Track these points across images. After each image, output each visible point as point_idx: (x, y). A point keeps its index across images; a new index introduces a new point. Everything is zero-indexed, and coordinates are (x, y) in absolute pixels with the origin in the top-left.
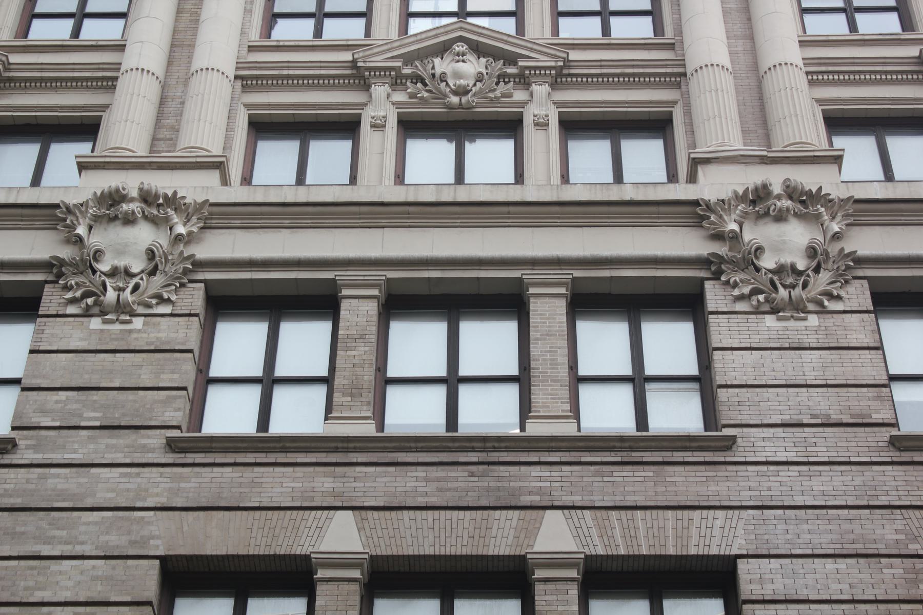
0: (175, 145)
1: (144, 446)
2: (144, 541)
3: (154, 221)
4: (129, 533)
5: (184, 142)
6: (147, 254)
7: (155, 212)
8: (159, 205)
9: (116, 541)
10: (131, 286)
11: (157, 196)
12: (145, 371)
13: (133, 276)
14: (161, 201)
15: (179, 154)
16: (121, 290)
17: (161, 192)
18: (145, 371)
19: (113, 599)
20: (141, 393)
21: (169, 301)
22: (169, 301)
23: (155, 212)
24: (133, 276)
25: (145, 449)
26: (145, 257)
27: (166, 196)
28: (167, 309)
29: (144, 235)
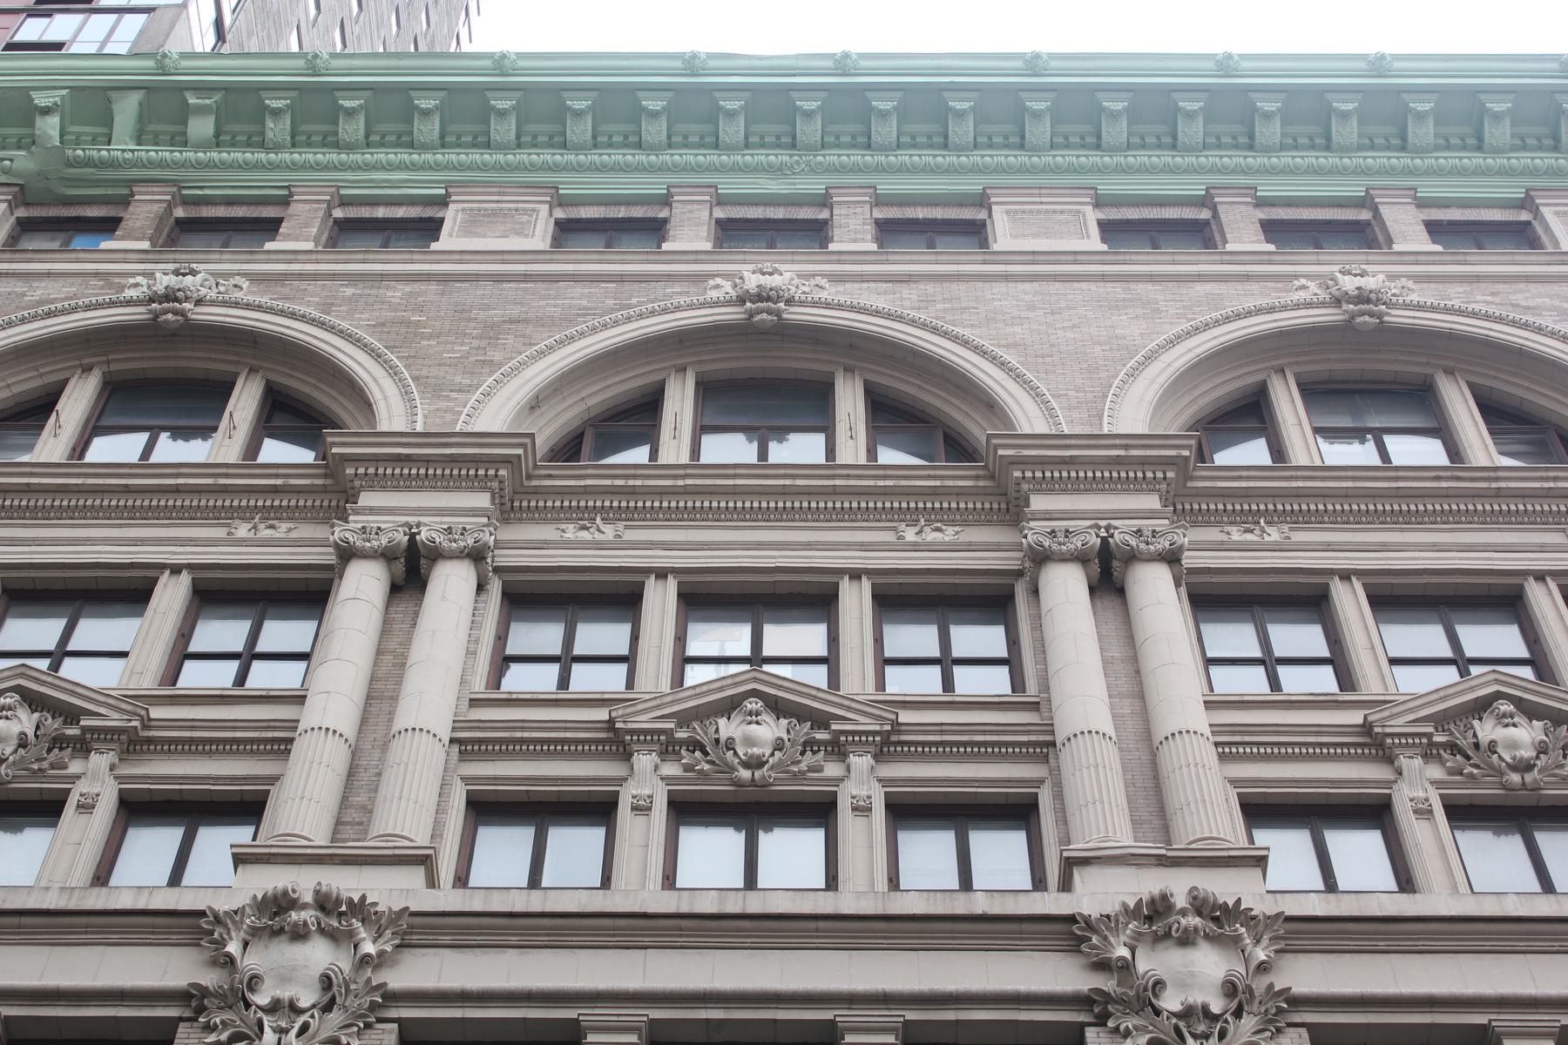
0: (366, 832)
3: (332, 936)
5: (377, 828)
6: (322, 981)
7: (336, 924)
8: (341, 914)
10: (297, 1026)
11: (338, 902)
13: (301, 1012)
14: (344, 908)
15: (370, 845)
16: (283, 1031)
17: (345, 895)
23: (336, 924)
24: (301, 1012)
26: (318, 986)
27: (351, 900)
29: (318, 956)
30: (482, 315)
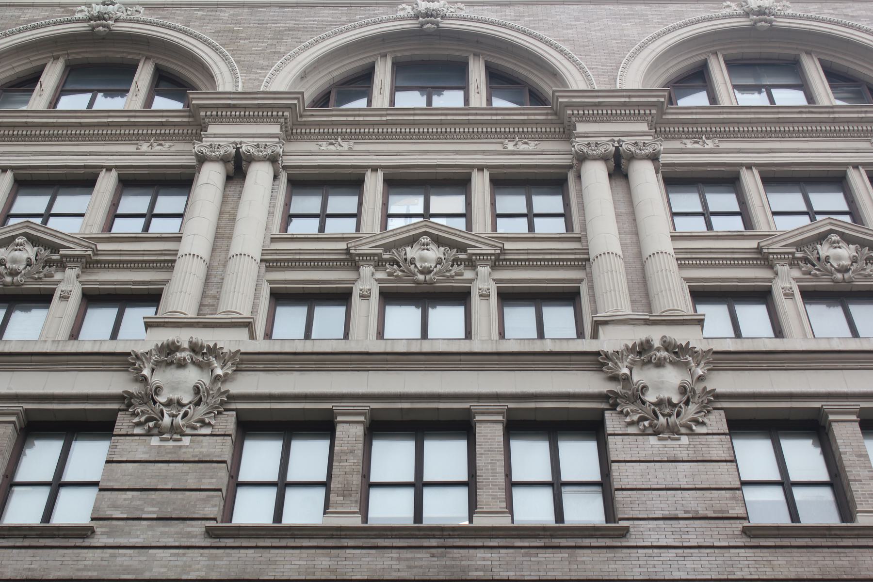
0: (216, 310)
1: (189, 533)
3: (199, 365)
5: (222, 308)
6: (194, 390)
7: (201, 359)
8: (203, 354)
10: (182, 413)
11: (202, 347)
12: (191, 477)
13: (183, 406)
14: (205, 351)
15: (219, 317)
16: (174, 416)
17: (205, 344)
18: (191, 477)
20: (187, 493)
21: (209, 424)
22: (209, 424)
23: (201, 359)
24: (183, 406)
25: (190, 535)
26: (192, 392)
27: (209, 347)
28: (207, 431)
29: (192, 376)
30: (273, 26)
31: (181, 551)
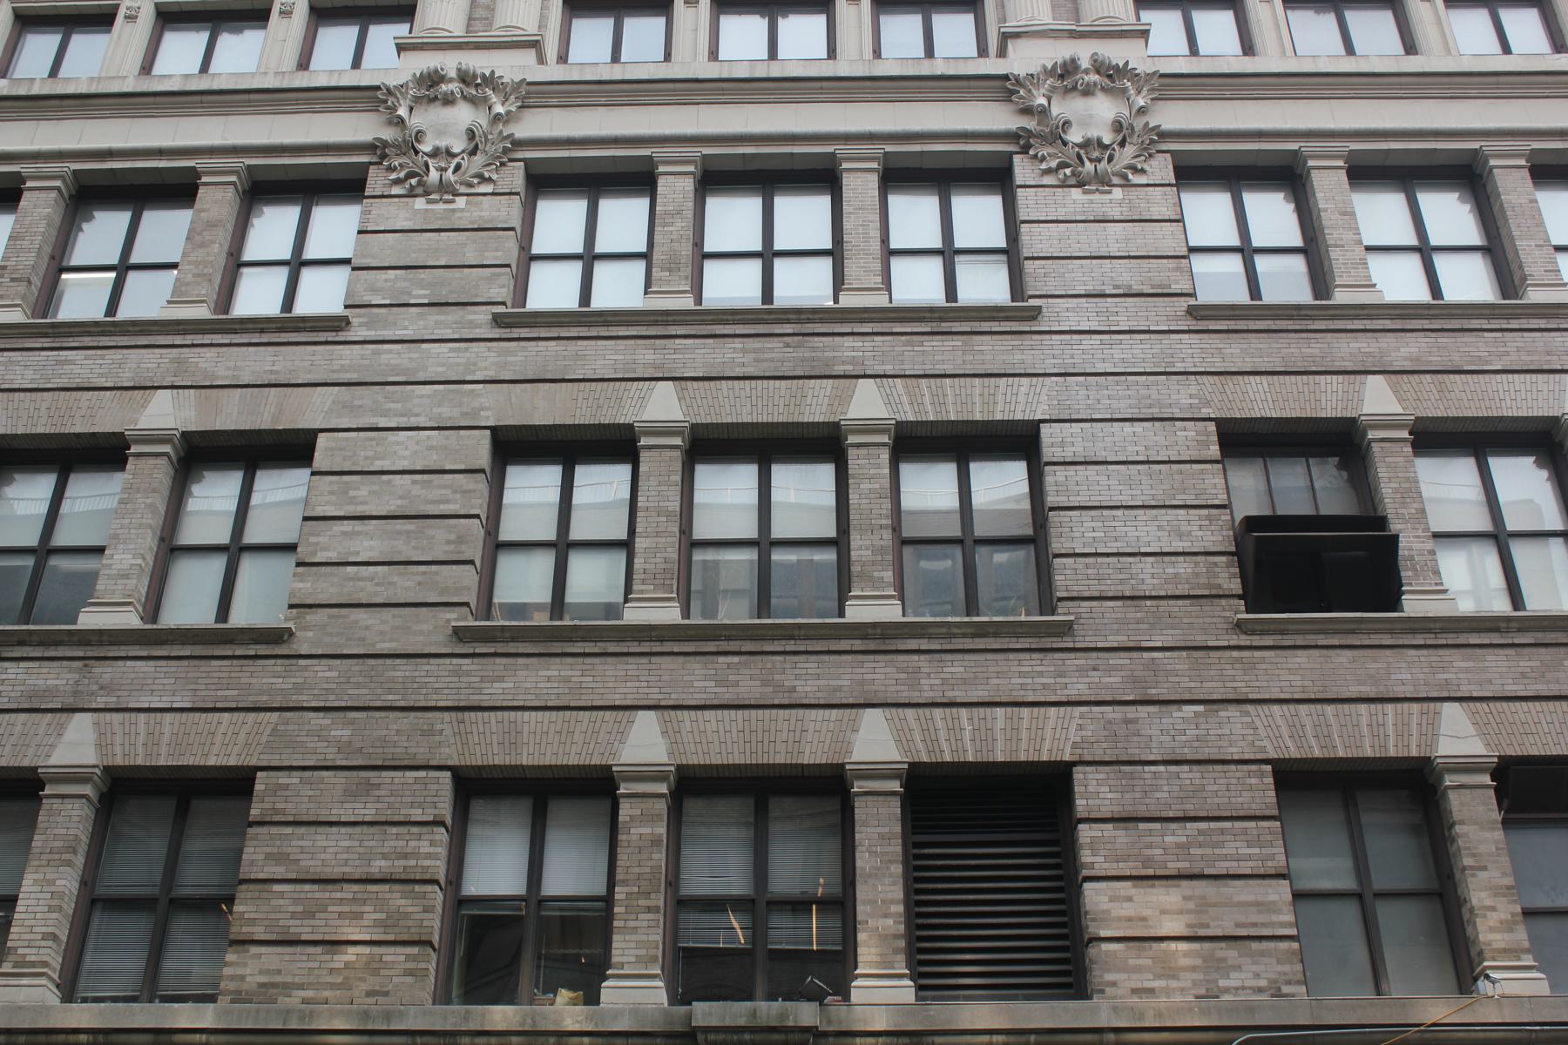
0: (491, 24)
1: (471, 322)
2: (475, 413)
4: (460, 405)
9: (448, 413)
10: (453, 166)
11: (475, 76)
13: (454, 156)
17: (479, 72)
19: (448, 467)
20: (466, 271)
21: (490, 180)
22: (490, 180)
24: (454, 156)
25: (472, 325)
26: (465, 137)
28: (488, 188)
29: (463, 116)
31: (462, 345)
